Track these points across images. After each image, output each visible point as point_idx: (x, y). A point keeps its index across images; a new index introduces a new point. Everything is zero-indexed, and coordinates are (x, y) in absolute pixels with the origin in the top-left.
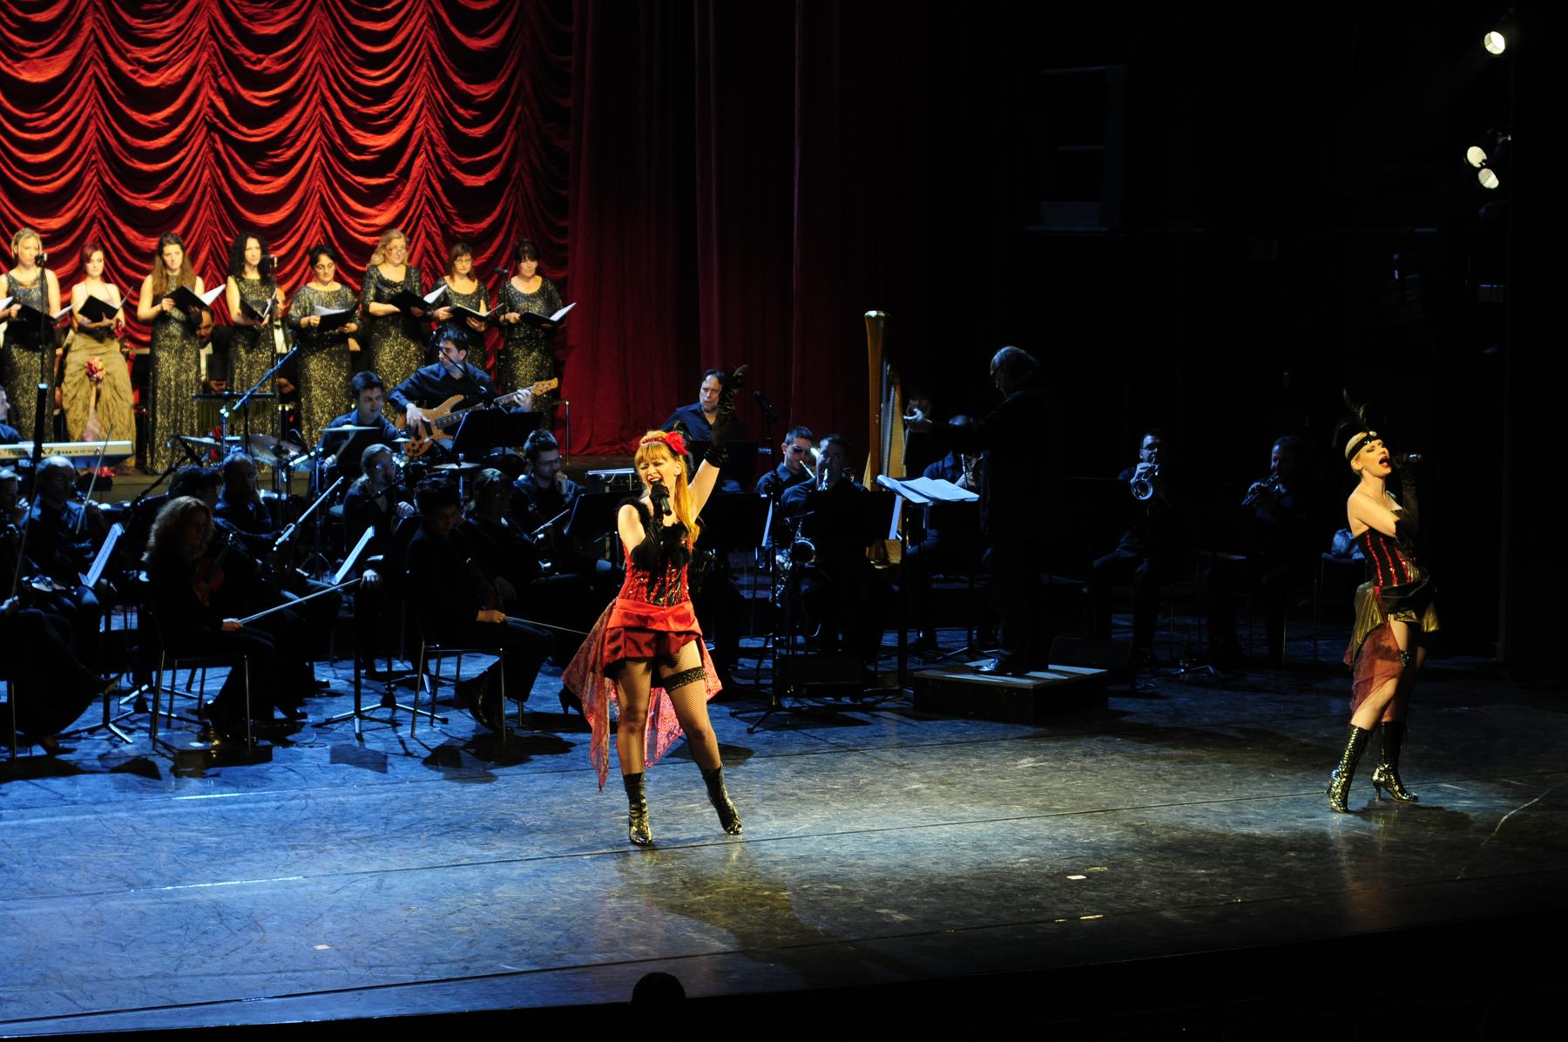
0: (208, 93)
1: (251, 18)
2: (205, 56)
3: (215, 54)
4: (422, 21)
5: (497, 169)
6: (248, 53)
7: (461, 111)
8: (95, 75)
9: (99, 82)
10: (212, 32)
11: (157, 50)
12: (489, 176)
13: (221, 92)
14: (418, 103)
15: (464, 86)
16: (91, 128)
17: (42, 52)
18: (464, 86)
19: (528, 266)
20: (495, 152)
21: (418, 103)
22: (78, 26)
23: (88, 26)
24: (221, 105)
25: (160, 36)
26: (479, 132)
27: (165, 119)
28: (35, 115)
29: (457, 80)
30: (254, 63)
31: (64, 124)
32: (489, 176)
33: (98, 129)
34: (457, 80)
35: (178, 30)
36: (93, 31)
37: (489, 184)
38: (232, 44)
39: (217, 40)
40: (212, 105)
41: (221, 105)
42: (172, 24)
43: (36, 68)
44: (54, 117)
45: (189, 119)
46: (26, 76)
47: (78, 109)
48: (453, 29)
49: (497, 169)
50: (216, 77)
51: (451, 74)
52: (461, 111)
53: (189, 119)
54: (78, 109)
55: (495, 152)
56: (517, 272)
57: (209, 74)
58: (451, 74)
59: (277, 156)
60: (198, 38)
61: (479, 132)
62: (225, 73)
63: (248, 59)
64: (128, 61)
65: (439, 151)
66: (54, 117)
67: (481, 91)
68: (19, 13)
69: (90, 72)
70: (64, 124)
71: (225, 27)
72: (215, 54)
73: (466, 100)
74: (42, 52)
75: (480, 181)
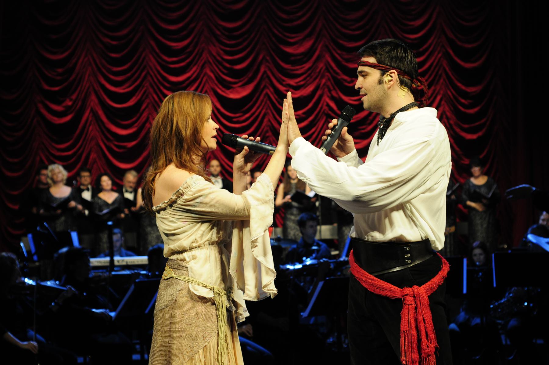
0: (326, 99)
1: (348, 61)
2: (324, 81)
3: (329, 79)
4: (440, 55)
5: (484, 130)
6: (345, 77)
7: (463, 101)
8: (267, 94)
9: (269, 97)
10: (327, 69)
11: (297, 80)
12: (480, 134)
13: (333, 98)
14: (439, 98)
15: (463, 88)
16: (266, 120)
17: (240, 84)
18: (463, 88)
19: (476, 170)
20: (482, 121)
21: (439, 98)
22: (257, 71)
23: (262, 70)
24: (332, 105)
25: (299, 72)
26: (472, 111)
27: (304, 113)
28: (237, 115)
29: (459, 85)
30: (349, 83)
31: (251, 119)
32: (480, 134)
33: (269, 121)
34: (459, 85)
35: (309, 69)
36: (265, 72)
37: (479, 138)
38: (337, 73)
39: (329, 72)
40: (328, 105)
41: (332, 105)
42: (307, 66)
43: (238, 92)
44: (247, 115)
45: (316, 112)
46: (232, 96)
47: (258, 111)
48: (456, 59)
49: (484, 130)
50: (330, 91)
51: (456, 81)
52: (463, 101)
53: (316, 112)
54: (258, 111)
55: (482, 121)
56: (471, 175)
57: (326, 90)
58: (456, 81)
59: (363, 129)
60: (320, 72)
61: (472, 111)
62: (335, 89)
63: (345, 81)
64: (281, 84)
65: (451, 122)
66: (247, 115)
67: (471, 90)
68: (228, 65)
69: (264, 92)
70: (251, 119)
71: (333, 65)
72: (329, 79)
73: (465, 95)
74: (240, 84)
75: (474, 137)
